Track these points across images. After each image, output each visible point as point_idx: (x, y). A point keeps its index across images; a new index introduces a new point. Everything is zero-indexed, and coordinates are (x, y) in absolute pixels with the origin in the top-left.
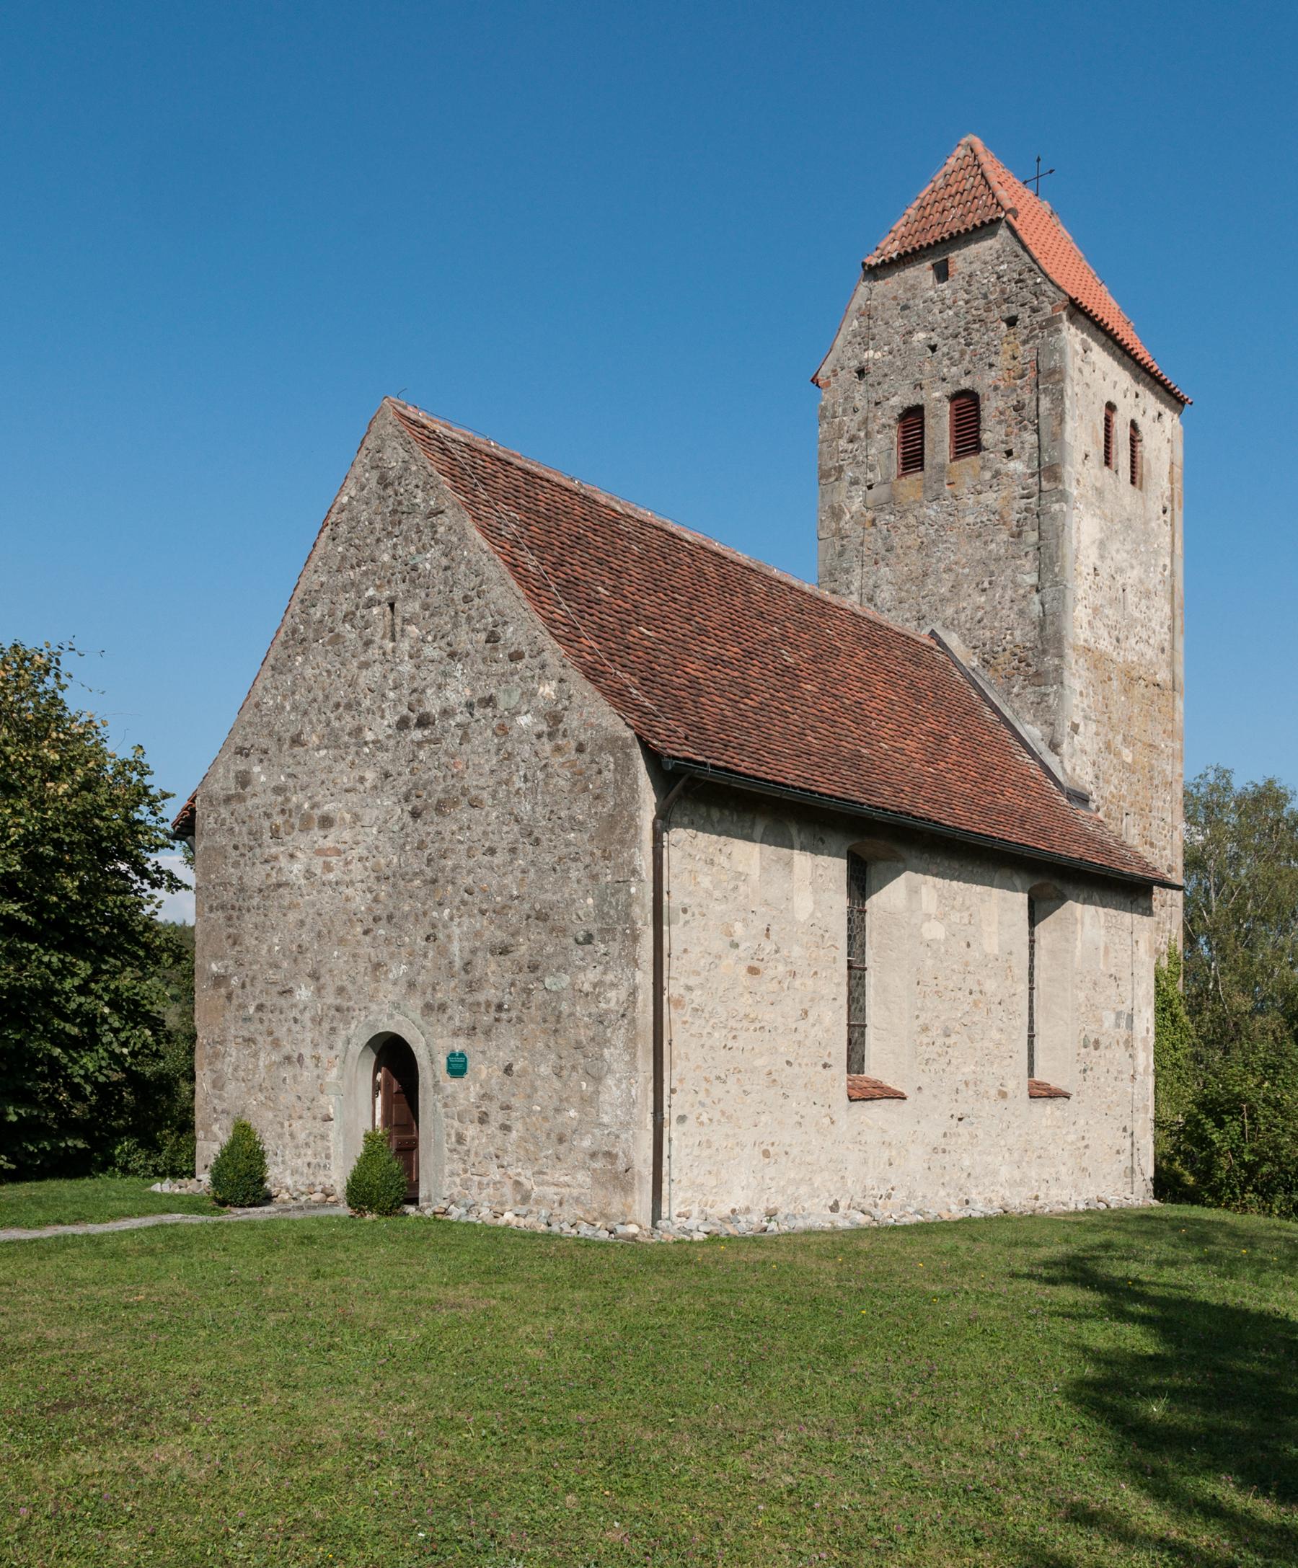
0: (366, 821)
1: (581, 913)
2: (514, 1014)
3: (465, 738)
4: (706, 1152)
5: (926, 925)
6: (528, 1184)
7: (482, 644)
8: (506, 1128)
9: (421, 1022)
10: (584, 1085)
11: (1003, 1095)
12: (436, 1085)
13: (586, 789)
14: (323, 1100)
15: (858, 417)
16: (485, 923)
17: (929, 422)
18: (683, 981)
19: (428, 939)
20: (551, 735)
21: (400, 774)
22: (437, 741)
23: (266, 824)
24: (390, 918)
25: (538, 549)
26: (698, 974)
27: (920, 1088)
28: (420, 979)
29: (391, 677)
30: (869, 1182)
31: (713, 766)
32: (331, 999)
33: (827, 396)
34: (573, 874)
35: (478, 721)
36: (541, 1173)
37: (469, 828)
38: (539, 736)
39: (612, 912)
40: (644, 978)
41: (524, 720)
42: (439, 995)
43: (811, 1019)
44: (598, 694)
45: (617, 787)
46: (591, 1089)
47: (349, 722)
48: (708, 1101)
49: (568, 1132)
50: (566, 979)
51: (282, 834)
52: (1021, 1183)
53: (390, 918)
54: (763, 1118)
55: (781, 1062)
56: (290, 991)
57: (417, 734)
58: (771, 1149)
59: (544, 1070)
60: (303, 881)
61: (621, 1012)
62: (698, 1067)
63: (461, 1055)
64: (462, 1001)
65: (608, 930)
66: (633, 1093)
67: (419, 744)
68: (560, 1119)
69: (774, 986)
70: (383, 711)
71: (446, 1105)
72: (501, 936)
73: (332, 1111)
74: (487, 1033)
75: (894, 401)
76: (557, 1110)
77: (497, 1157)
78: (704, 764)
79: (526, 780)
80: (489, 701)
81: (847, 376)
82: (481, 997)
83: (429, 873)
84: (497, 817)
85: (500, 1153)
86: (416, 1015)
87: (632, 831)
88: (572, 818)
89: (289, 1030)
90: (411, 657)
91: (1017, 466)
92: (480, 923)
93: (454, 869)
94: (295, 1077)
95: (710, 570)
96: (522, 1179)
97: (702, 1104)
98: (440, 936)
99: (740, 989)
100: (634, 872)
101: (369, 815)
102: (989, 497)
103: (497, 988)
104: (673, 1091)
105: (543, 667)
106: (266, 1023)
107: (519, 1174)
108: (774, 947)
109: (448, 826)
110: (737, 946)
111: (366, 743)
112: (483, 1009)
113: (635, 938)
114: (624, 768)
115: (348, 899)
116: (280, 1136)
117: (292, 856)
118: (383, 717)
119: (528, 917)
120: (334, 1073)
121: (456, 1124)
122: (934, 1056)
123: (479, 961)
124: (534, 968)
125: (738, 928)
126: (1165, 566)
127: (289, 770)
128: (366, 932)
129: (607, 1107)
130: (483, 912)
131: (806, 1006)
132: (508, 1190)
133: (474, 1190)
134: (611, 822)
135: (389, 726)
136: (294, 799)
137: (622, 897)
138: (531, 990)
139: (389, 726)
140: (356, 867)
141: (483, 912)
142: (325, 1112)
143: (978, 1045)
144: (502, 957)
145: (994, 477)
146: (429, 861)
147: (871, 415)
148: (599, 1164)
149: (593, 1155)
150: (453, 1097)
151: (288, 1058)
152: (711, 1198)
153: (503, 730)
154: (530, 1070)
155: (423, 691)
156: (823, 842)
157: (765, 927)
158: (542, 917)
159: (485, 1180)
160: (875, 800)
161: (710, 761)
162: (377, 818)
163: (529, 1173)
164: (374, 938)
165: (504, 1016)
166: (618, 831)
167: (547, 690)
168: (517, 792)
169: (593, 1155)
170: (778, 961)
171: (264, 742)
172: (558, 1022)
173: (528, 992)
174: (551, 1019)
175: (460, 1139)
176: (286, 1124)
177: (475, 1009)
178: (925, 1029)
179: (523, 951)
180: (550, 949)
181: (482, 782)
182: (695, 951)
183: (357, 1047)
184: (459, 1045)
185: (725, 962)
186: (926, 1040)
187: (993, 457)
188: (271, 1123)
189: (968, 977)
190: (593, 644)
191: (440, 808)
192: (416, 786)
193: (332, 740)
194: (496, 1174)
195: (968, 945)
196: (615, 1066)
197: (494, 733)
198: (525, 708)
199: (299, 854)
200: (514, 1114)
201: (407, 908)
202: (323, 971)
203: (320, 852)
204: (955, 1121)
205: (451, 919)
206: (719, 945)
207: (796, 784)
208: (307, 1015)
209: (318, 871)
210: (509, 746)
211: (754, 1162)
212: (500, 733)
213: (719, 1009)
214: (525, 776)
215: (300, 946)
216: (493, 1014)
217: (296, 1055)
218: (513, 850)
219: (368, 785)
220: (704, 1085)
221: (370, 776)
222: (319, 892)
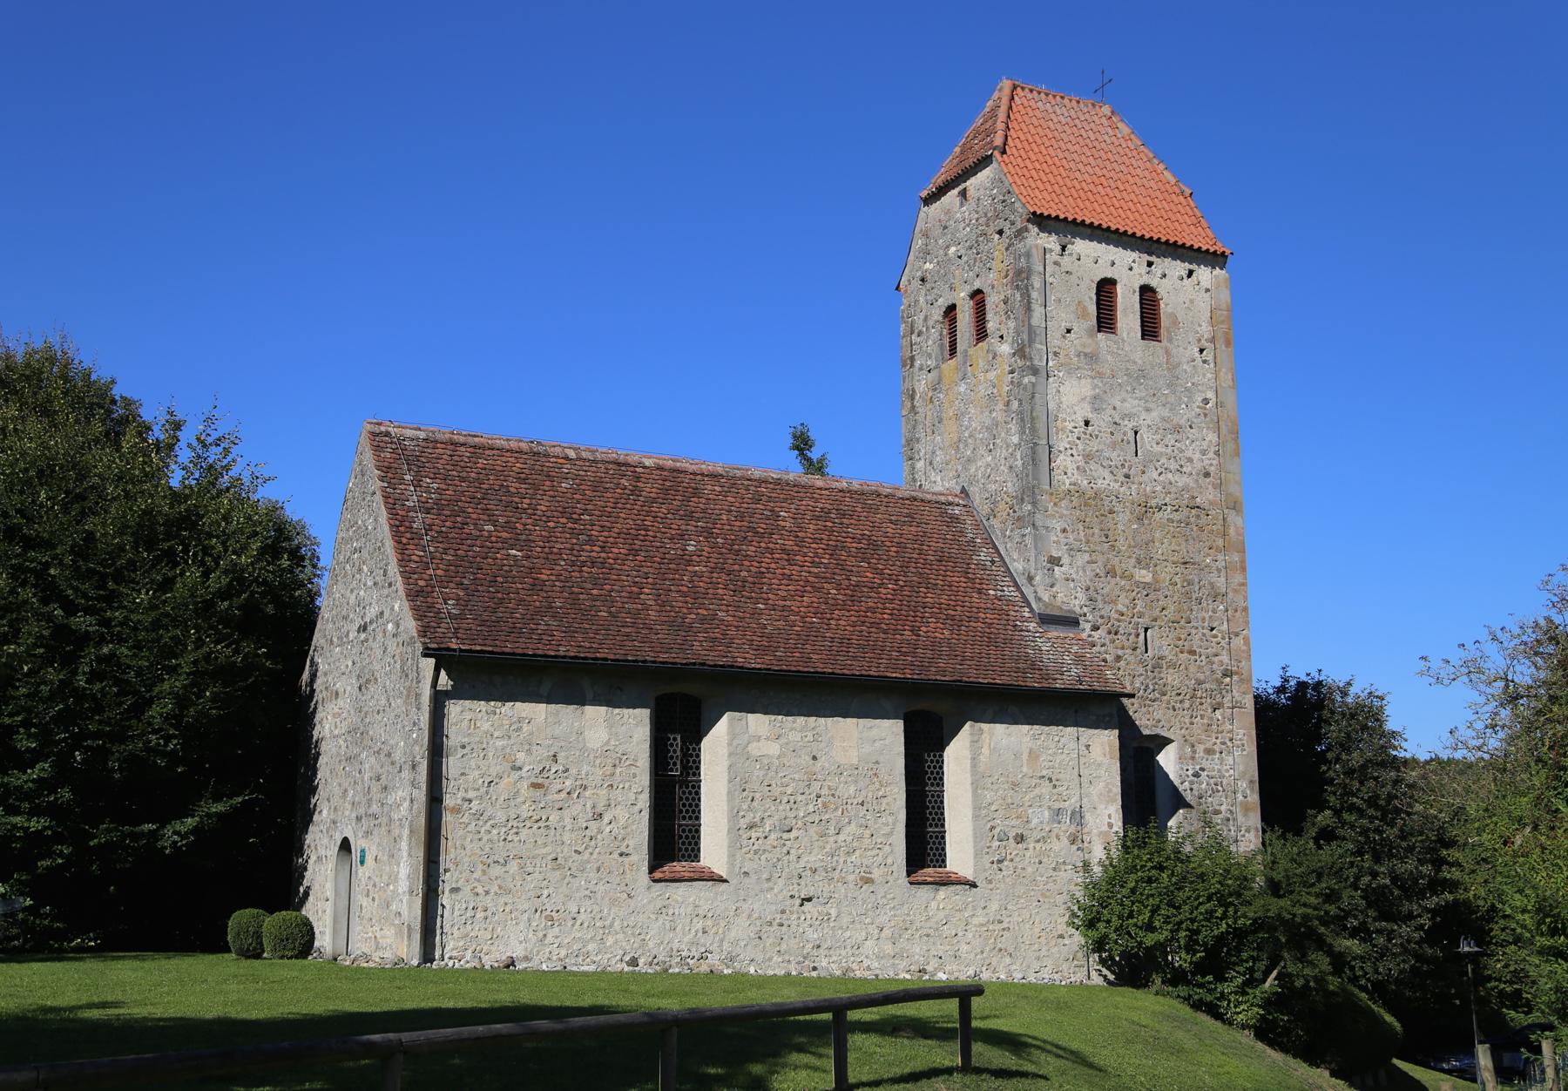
15: (922, 316)
17: (959, 316)
43: (606, 819)
81: (916, 283)
126: (1206, 401)
131: (599, 809)
185: (506, 780)
187: (992, 340)
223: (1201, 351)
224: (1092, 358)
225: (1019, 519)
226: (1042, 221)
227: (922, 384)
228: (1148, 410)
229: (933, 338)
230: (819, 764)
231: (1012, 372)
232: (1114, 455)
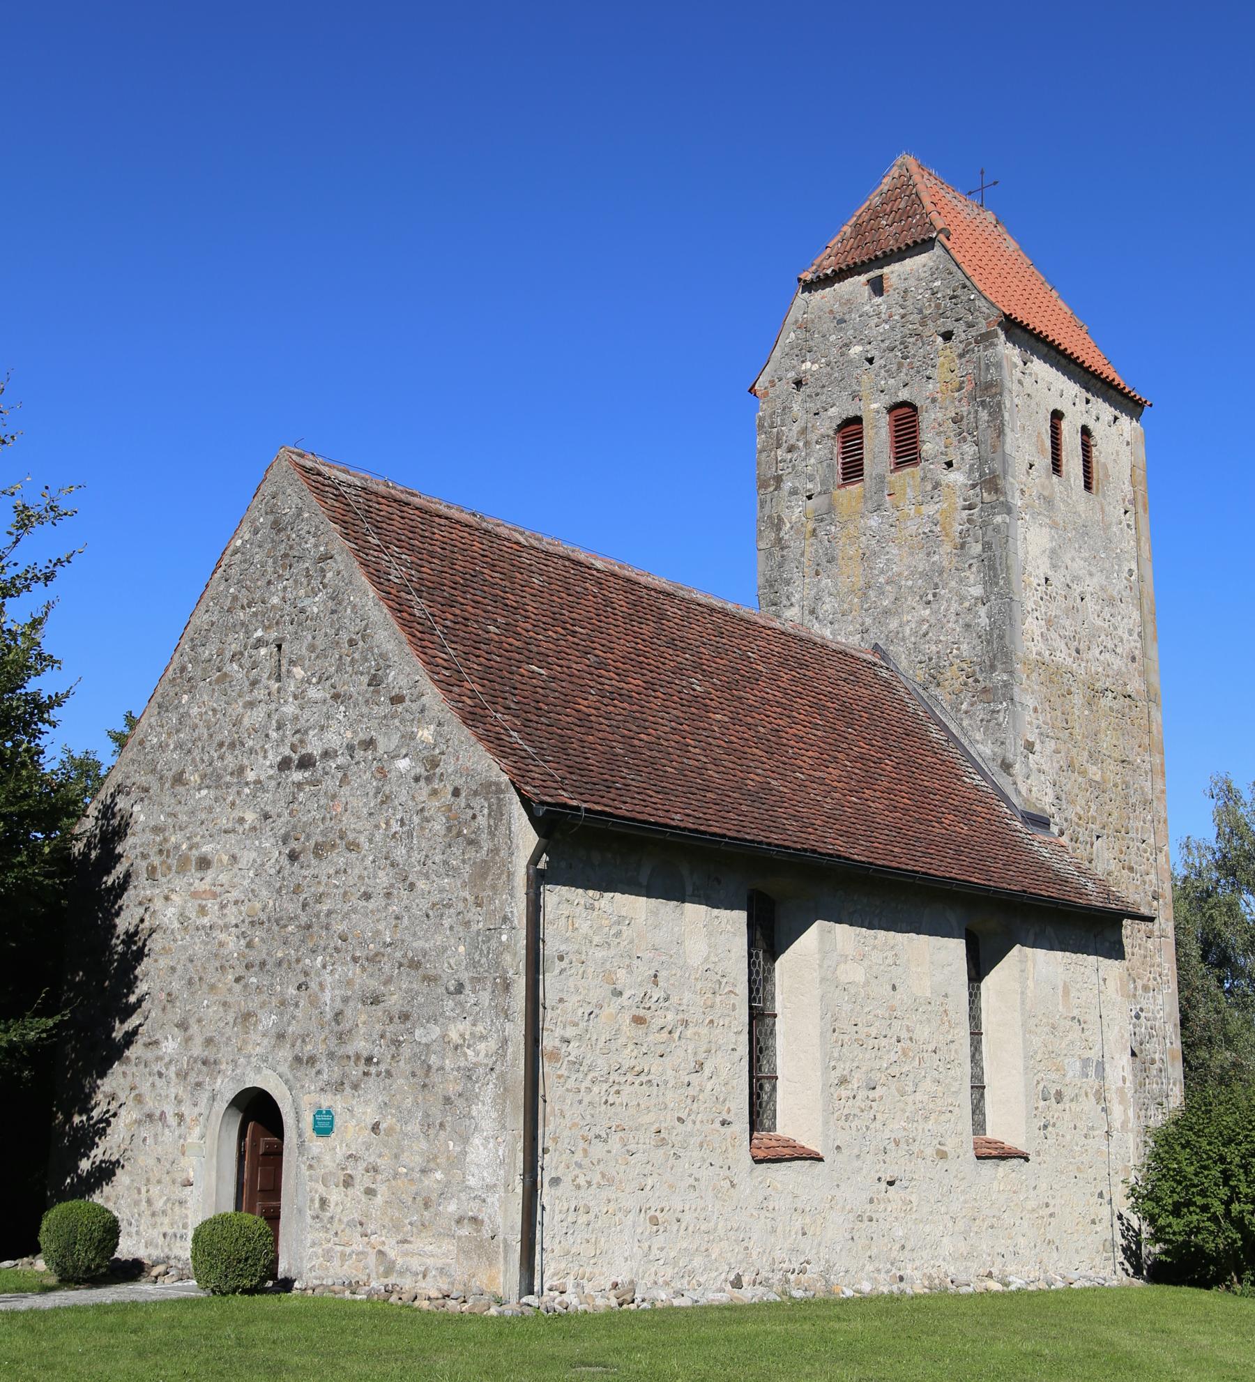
0: (243, 863)
1: (452, 961)
2: (382, 1067)
3: (344, 780)
4: (583, 1219)
5: (842, 967)
6: (392, 1254)
7: (365, 687)
8: (370, 1192)
9: (290, 1077)
10: (451, 1144)
11: (942, 1155)
12: (301, 1145)
13: (459, 834)
14: (184, 1162)
15: (796, 428)
16: (358, 970)
17: (868, 432)
18: (558, 1032)
19: (299, 987)
20: (428, 779)
21: (279, 816)
22: (315, 783)
23: (144, 864)
24: (263, 964)
25: (425, 589)
26: (576, 1025)
27: (838, 1147)
28: (290, 1029)
29: (275, 717)
30: (778, 1254)
31: (587, 810)
32: (197, 1050)
33: (765, 407)
34: (447, 922)
36: (405, 1241)
37: (345, 871)
38: (417, 779)
39: (483, 960)
40: (517, 1030)
41: (403, 764)
42: (309, 1047)
44: (474, 739)
45: (490, 833)
46: (458, 1149)
47: (231, 761)
48: (586, 1162)
49: (434, 1196)
50: (436, 1031)
51: (159, 876)
52: (968, 1257)
53: (263, 964)
54: (650, 1182)
55: (669, 1120)
56: (156, 1043)
57: (297, 776)
58: (658, 1214)
59: (414, 1127)
60: (176, 925)
62: (575, 1125)
63: (328, 1112)
65: (478, 980)
66: (500, 1153)
67: (299, 786)
69: (664, 1035)
70: (266, 752)
71: (311, 1167)
72: (373, 984)
74: (355, 1087)
75: (833, 411)
77: (361, 1224)
78: (577, 808)
79: (403, 824)
80: (369, 744)
82: (350, 1049)
83: (304, 919)
84: (374, 861)
85: (364, 1220)
86: (284, 1068)
87: (504, 877)
88: (445, 863)
89: (153, 1085)
90: (295, 697)
91: (957, 478)
92: (354, 971)
93: (329, 913)
94: (156, 1135)
95: (619, 600)
96: (386, 1249)
97: (579, 1165)
98: (314, 986)
99: (622, 1040)
100: (505, 919)
101: (247, 857)
102: (929, 509)
103: (367, 1040)
104: (545, 1151)
105: (422, 711)
106: (130, 1078)
107: (384, 1243)
108: (662, 995)
109: (326, 869)
110: (621, 993)
111: (247, 784)
113: (507, 987)
114: (497, 813)
115: (221, 944)
116: (137, 1203)
117: (167, 898)
118: (265, 757)
119: (401, 965)
121: (321, 1188)
122: (857, 1111)
123: (348, 1012)
124: (405, 1017)
125: (622, 973)
126: (1131, 572)
127: (168, 810)
128: (238, 980)
129: (473, 1169)
130: (355, 960)
132: (372, 1259)
133: (336, 1262)
134: (482, 870)
135: (271, 767)
136: (173, 839)
137: (494, 944)
138: (400, 1043)
139: (271, 767)
140: (231, 910)
141: (355, 960)
143: (910, 1099)
144: (374, 1007)
145: (935, 488)
146: (304, 906)
147: (810, 425)
148: (465, 1231)
149: (459, 1221)
150: (318, 1159)
151: (150, 1116)
152: (589, 1270)
153: (382, 773)
154: (398, 1128)
155: (306, 732)
156: (719, 882)
157: (652, 972)
158: (415, 965)
159: (348, 1250)
160: (775, 838)
161: (585, 805)
162: (254, 861)
164: (246, 986)
165: (373, 1070)
166: (490, 878)
167: (426, 734)
168: (394, 836)
169: (459, 1221)
170: (668, 1009)
171: (142, 779)
172: (427, 1075)
173: (397, 1043)
175: (323, 1202)
176: (144, 1190)
177: (345, 1062)
178: (843, 1081)
179: (394, 1001)
180: (421, 999)
181: (359, 826)
182: (572, 1001)
183: (222, 1105)
184: (326, 1101)
186: (844, 1094)
188: (129, 1188)
189: (895, 1023)
190: (474, 686)
191: (319, 851)
192: (294, 827)
193: (213, 780)
194: (358, 1244)
195: (894, 988)
196: (483, 1124)
197: (373, 776)
198: (404, 752)
199: (173, 897)
200: (379, 1177)
201: (280, 955)
202: (192, 1021)
203: (195, 895)
204: (884, 1185)
205: (324, 967)
206: (599, 992)
207: (682, 824)
208: (173, 1068)
209: (193, 915)
210: (387, 789)
211: (639, 1230)
212: (379, 776)
213: (599, 1062)
214: (402, 820)
215: (169, 994)
216: (362, 1067)
217: (158, 1114)
218: (388, 895)
219: (247, 826)
220: (581, 1144)
221: (250, 817)
222: (192, 937)
223: (1126, 512)
224: (1048, 501)
225: (985, 690)
226: (1014, 328)
227: (795, 512)
228: (1091, 575)
229: (825, 454)
230: (898, 995)
231: (970, 507)
232: (1067, 623)
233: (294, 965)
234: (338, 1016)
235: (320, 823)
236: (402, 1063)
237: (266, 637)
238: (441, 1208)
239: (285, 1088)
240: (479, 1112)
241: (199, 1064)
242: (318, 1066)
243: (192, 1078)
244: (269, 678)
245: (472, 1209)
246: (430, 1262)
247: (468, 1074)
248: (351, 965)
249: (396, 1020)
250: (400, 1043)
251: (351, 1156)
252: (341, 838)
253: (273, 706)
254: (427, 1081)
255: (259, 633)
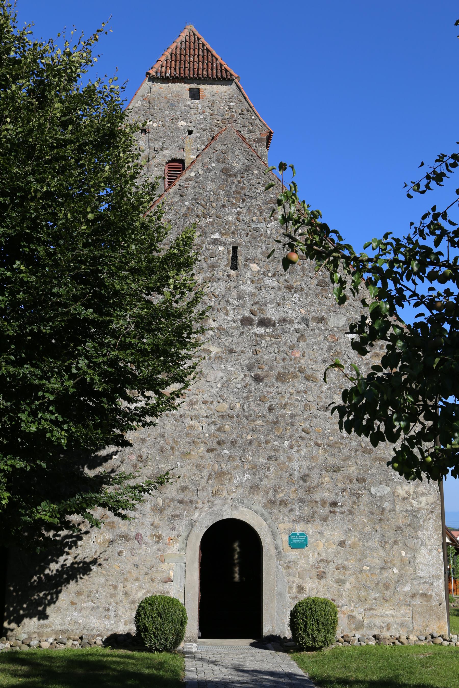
10: (404, 553)
14: (164, 566)
16: (321, 451)
19: (270, 458)
28: (263, 484)
35: (313, 330)
42: (281, 495)
49: (392, 584)
50: (387, 490)
59: (374, 543)
61: (430, 509)
64: (301, 500)
68: (385, 574)
72: (332, 460)
73: (172, 574)
76: (383, 568)
82: (317, 497)
84: (330, 389)
86: (259, 508)
90: (252, 282)
93: (293, 416)
96: (355, 614)
107: (353, 611)
109: (286, 389)
112: (319, 505)
120: (177, 546)
123: (315, 476)
130: (318, 445)
138: (360, 495)
141: (318, 445)
142: (165, 575)
146: (270, 410)
149: (413, 596)
155: (265, 304)
163: (361, 610)
165: (338, 510)
174: (376, 512)
176: (120, 586)
180: (374, 471)
181: (315, 367)
197: (325, 338)
200: (348, 572)
205: (291, 447)
212: (331, 339)
216: (328, 508)
217: (133, 535)
233: (263, 445)
234: (304, 478)
235: (281, 361)
236: (361, 507)
237: (223, 240)
238: (398, 589)
239: (261, 520)
240: (424, 535)
241: (175, 503)
242: (290, 506)
243: (169, 512)
244: (226, 266)
245: (422, 589)
246: (390, 620)
247: (414, 514)
248: (315, 448)
249: (355, 481)
250: (360, 495)
251: (322, 560)
252: (301, 372)
253: (232, 284)
254: (382, 517)
255: (217, 236)
